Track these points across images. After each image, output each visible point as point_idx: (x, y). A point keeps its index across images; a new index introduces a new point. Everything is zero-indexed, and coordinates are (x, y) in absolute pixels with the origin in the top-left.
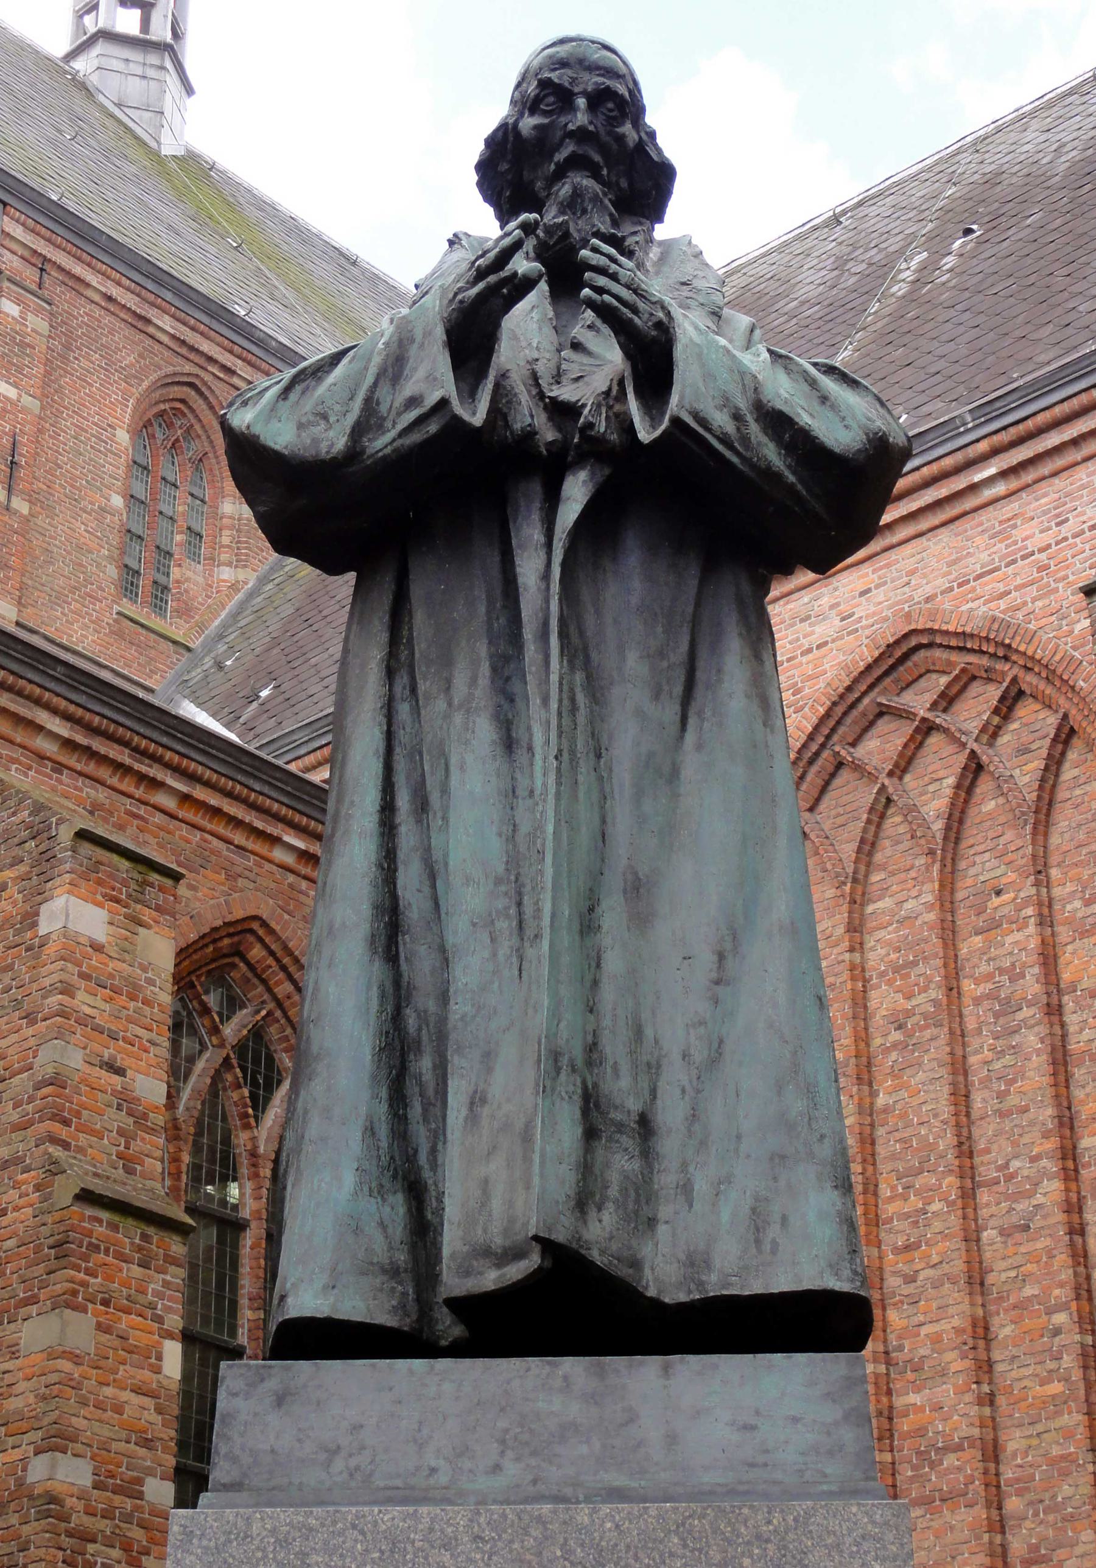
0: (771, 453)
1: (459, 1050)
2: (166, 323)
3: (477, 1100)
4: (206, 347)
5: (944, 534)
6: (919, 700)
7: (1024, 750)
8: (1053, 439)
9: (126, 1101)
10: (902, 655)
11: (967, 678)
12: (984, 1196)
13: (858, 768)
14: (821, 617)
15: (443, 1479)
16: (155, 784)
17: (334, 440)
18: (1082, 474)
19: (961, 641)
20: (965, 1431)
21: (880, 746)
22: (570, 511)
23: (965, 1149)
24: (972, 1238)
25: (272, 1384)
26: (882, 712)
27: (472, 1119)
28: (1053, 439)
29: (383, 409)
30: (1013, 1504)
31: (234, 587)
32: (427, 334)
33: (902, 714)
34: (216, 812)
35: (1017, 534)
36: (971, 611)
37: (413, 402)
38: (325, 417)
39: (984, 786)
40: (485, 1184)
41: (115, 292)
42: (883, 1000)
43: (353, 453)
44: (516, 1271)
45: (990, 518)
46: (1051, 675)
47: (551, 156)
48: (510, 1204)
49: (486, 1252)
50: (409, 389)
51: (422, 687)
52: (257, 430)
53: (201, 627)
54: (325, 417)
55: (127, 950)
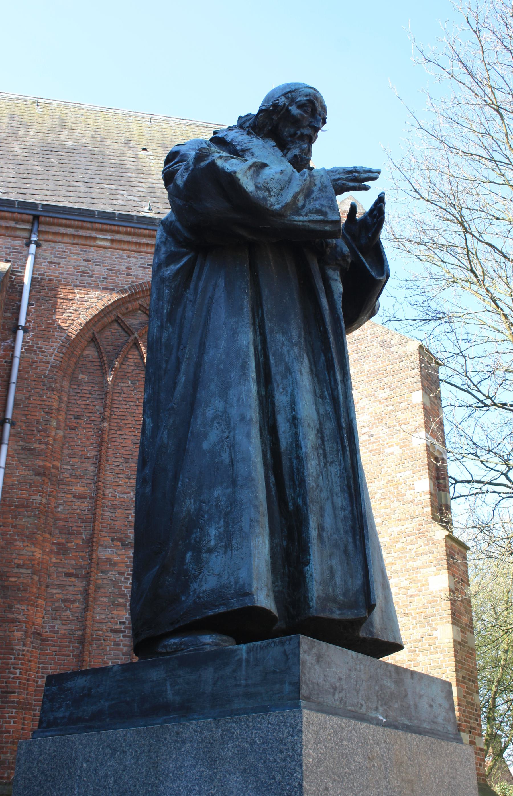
3: (321, 528)
15: (364, 710)
17: (275, 203)
25: (315, 650)
27: (320, 536)
29: (300, 204)
37: (319, 212)
38: (269, 190)
40: (331, 570)
43: (279, 214)
47: (299, 128)
48: (345, 582)
49: (335, 600)
51: (268, 325)
52: (239, 176)
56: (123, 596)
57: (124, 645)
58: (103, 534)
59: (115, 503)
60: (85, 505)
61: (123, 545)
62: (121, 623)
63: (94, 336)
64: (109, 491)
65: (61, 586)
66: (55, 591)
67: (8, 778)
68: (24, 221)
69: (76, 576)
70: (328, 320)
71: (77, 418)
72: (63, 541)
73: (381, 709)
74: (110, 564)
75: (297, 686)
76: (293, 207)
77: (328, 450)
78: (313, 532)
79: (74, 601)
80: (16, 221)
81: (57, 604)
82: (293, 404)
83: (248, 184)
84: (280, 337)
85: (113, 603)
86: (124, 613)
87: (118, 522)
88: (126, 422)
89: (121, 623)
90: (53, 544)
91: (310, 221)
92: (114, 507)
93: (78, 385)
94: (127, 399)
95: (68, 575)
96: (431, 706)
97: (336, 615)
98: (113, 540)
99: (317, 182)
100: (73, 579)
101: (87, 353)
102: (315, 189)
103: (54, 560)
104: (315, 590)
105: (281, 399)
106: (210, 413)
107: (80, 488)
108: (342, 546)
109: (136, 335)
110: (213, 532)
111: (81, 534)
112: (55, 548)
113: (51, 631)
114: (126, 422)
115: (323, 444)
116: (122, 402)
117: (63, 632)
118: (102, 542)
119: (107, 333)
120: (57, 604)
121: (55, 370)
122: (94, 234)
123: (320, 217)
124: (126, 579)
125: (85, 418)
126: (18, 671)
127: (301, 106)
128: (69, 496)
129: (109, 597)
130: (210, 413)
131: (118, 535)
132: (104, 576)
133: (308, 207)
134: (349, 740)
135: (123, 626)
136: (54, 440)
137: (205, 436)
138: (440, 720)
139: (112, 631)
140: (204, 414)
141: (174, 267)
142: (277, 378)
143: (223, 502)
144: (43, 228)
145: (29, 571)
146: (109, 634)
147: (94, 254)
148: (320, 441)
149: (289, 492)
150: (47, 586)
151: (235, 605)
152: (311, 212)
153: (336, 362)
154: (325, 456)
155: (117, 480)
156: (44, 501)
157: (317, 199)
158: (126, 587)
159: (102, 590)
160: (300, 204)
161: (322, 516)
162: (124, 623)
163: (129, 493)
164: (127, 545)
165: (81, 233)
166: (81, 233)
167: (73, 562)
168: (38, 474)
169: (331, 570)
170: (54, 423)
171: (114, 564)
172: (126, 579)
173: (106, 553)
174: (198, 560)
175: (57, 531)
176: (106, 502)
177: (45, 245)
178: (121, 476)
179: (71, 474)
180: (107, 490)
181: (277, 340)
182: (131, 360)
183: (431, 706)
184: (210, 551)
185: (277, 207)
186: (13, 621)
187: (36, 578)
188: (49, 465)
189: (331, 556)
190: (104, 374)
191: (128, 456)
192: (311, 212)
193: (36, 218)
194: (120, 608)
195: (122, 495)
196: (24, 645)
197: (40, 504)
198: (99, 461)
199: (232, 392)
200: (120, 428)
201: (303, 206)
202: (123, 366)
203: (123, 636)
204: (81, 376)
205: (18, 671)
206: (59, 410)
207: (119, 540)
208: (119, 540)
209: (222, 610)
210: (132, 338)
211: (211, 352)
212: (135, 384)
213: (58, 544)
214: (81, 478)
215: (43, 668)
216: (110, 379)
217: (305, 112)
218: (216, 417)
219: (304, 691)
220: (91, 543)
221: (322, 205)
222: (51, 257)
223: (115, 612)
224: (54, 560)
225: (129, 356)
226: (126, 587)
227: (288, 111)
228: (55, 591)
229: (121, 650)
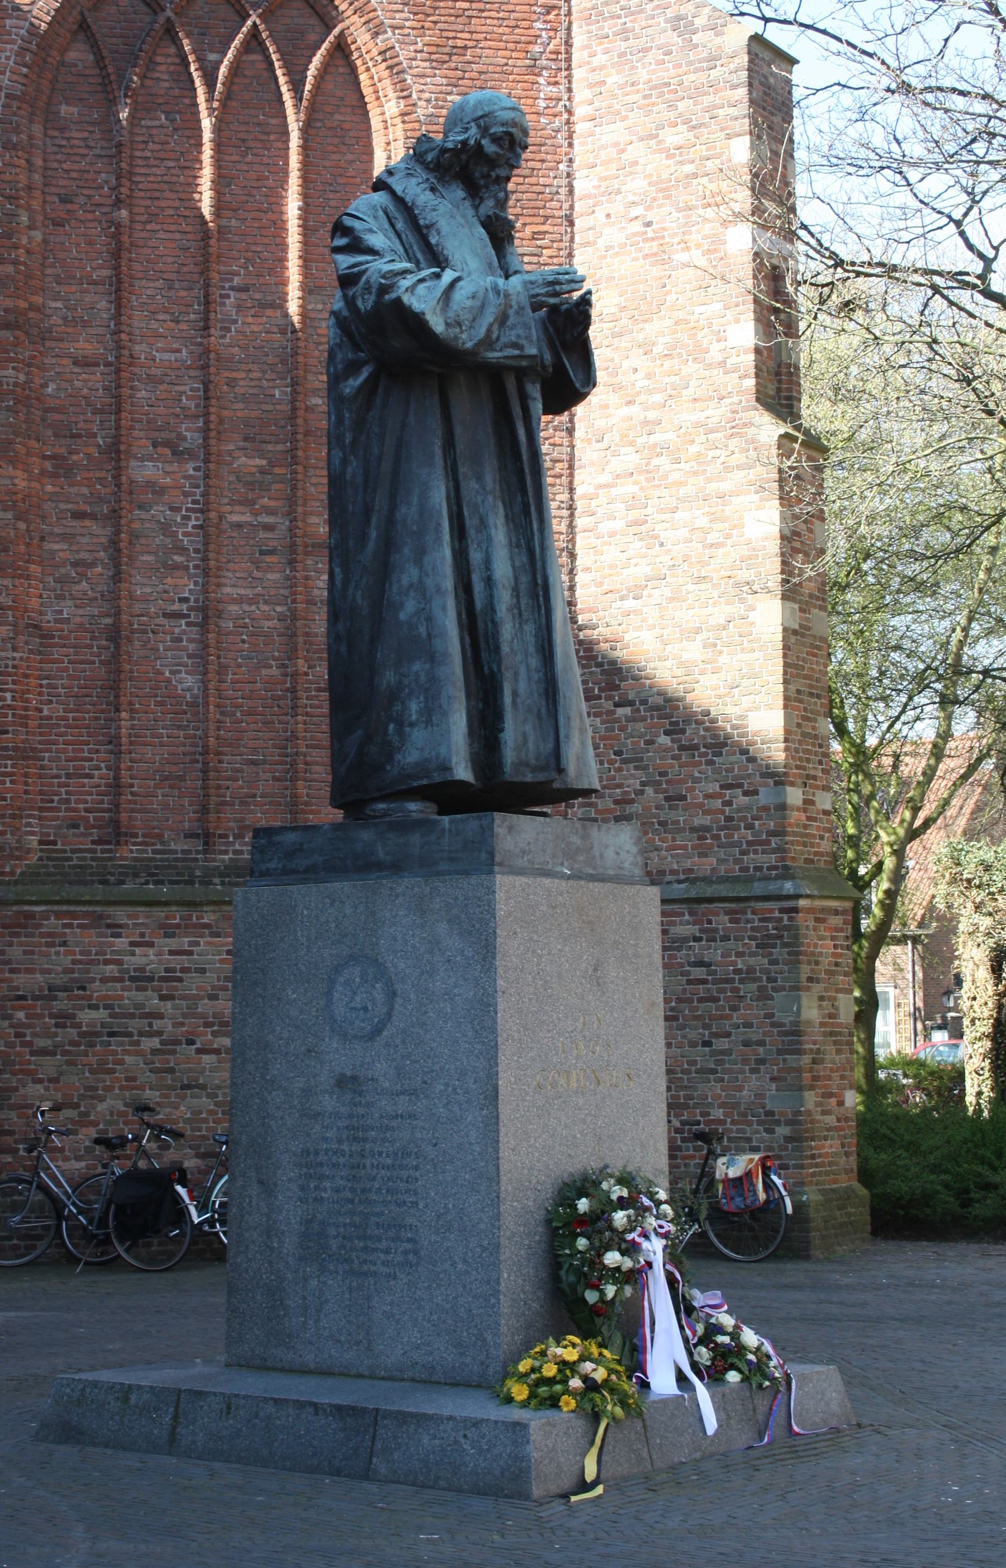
1: (507, 669)
3: (515, 694)
15: (550, 867)
17: (467, 340)
25: (507, 823)
27: (514, 703)
29: (494, 336)
32: (522, 308)
37: (515, 345)
40: (525, 735)
43: (473, 353)
49: (527, 764)
51: (462, 470)
52: (428, 317)
54: (459, 324)
56: (182, 550)
57: (191, 641)
58: (136, 433)
59: (154, 371)
60: (97, 379)
61: (174, 453)
62: (182, 600)
63: (84, 20)
65: (66, 538)
66: (56, 547)
67: (12, 873)
69: (93, 516)
70: (525, 456)
71: (65, 200)
72: (63, 451)
73: (566, 863)
74: (154, 492)
75: (492, 854)
76: (488, 342)
77: (523, 606)
78: (508, 700)
79: (93, 565)
81: (63, 571)
82: (488, 562)
83: (437, 324)
84: (474, 484)
85: (165, 564)
86: (185, 580)
87: (162, 410)
88: (163, 204)
89: (182, 600)
90: (45, 458)
91: (505, 357)
92: (153, 380)
93: (62, 129)
94: (162, 155)
95: (78, 515)
96: (618, 854)
97: (529, 778)
98: (155, 445)
99: (514, 303)
100: (87, 523)
101: (72, 55)
102: (511, 312)
103: (49, 488)
104: (509, 756)
105: (476, 557)
106: (405, 581)
107: (84, 345)
108: (535, 710)
109: (169, 13)
110: (414, 707)
111: (95, 435)
112: (48, 465)
113: (56, 621)
114: (163, 204)
115: (519, 602)
116: (152, 162)
117: (78, 620)
118: (135, 449)
120: (63, 571)
121: (15, 104)
123: (516, 352)
124: (184, 518)
125: (82, 200)
126: (8, 695)
127: (496, 139)
128: (65, 361)
129: (156, 553)
130: (405, 581)
131: (165, 435)
132: (143, 515)
133: (504, 339)
134: (534, 894)
135: (185, 606)
136: (28, 252)
137: (402, 605)
138: (627, 865)
139: (166, 615)
140: (399, 581)
141: (354, 383)
142: (471, 533)
143: (423, 678)
145: (9, 515)
146: (162, 620)
148: (515, 601)
149: (484, 655)
150: (42, 539)
151: (437, 778)
152: (506, 346)
153: (533, 508)
154: (520, 614)
155: (154, 325)
156: (22, 378)
157: (513, 327)
158: (186, 534)
159: (143, 541)
160: (494, 336)
161: (516, 681)
162: (186, 600)
163: (179, 351)
164: (182, 453)
167: (85, 490)
169: (525, 735)
170: (24, 219)
171: (161, 491)
172: (184, 518)
173: (145, 470)
174: (400, 732)
175: (49, 432)
176: (137, 370)
178: (161, 317)
179: (65, 318)
180: (137, 347)
181: (470, 487)
182: (163, 68)
183: (618, 854)
184: (412, 725)
185: (469, 345)
187: (22, 525)
188: (23, 304)
189: (525, 721)
190: (111, 104)
191: (174, 276)
192: (506, 346)
194: (178, 573)
195: (166, 356)
196: (15, 649)
197: (16, 384)
198: (118, 291)
199: (426, 559)
200: (153, 217)
201: (498, 339)
202: (148, 82)
203: (188, 624)
204: (64, 110)
205: (8, 695)
206: (29, 188)
207: (167, 444)
208: (167, 444)
209: (425, 782)
210: (162, 19)
211: (403, 509)
212: (174, 120)
213: (53, 457)
214: (86, 324)
215: (50, 686)
216: (124, 115)
217: (501, 147)
218: (411, 586)
219: (498, 858)
220: (116, 453)
221: (518, 336)
223: (169, 580)
224: (49, 488)
225: (159, 59)
226: (186, 534)
227: (479, 145)
228: (56, 547)
229: (185, 649)
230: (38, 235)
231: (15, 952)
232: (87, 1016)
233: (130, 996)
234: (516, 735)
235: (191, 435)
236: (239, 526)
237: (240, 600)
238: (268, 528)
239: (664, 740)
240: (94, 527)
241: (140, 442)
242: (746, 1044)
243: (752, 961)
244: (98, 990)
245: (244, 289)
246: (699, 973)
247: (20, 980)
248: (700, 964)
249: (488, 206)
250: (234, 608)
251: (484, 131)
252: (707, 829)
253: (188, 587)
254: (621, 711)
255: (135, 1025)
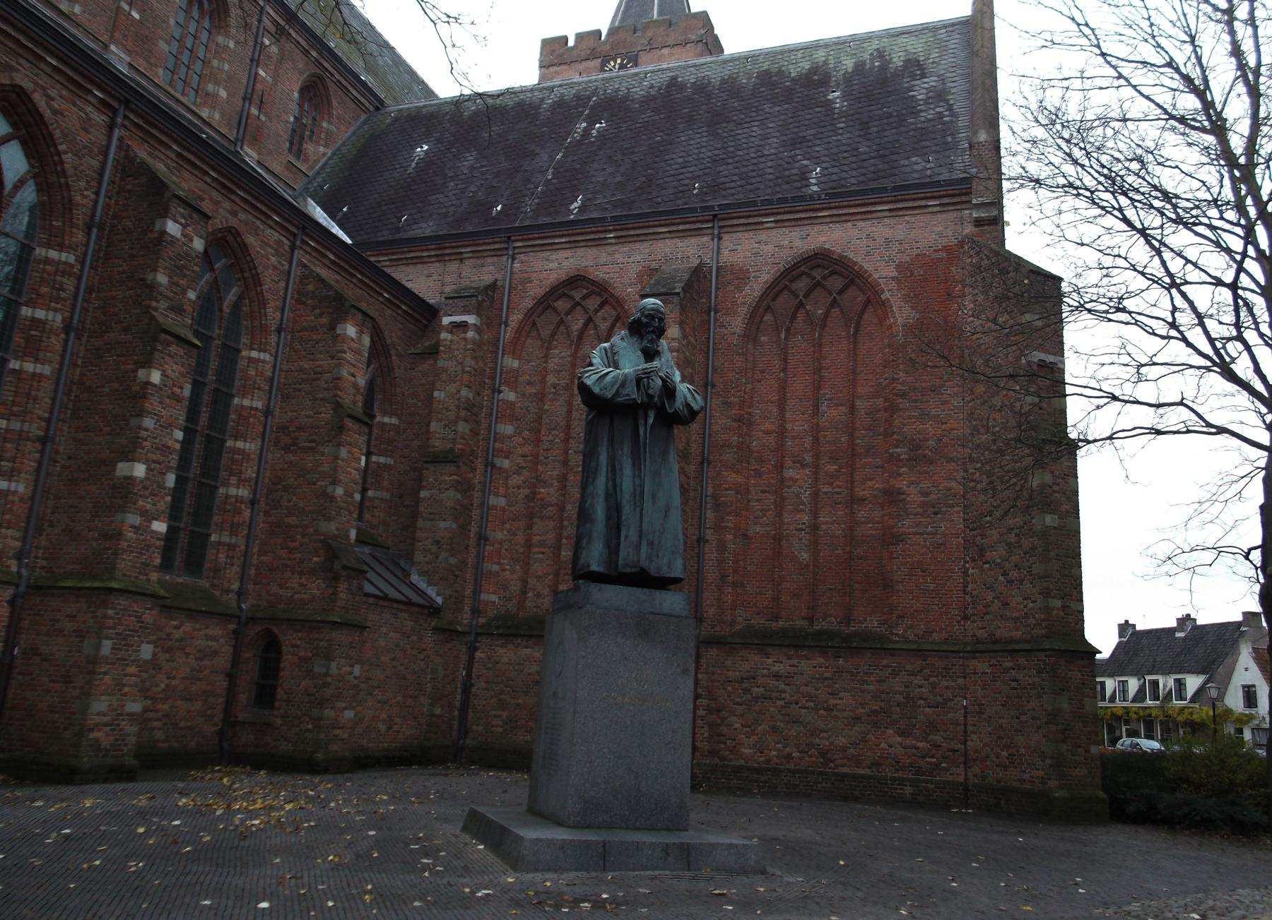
0: (686, 412)
2: (314, 54)
3: (627, 536)
4: (326, 65)
5: (594, 249)
6: (577, 296)
7: (605, 319)
8: (632, 232)
9: (355, 385)
10: (576, 280)
11: (592, 293)
12: (571, 441)
13: (555, 310)
14: (552, 261)
16: (353, 276)
17: (609, 395)
18: (638, 245)
19: (593, 282)
20: (555, 501)
21: (562, 305)
22: (651, 421)
23: (568, 427)
24: (566, 452)
26: (565, 295)
28: (632, 232)
30: (566, 523)
31: (324, 154)
33: (572, 298)
34: (368, 285)
35: (617, 256)
36: (599, 274)
39: (591, 325)
41: (300, 39)
42: (551, 379)
44: (634, 570)
45: (609, 249)
46: (617, 300)
50: (626, 392)
53: (312, 168)
55: (359, 339)
56: (804, 504)
64: (789, 426)
68: (707, 221)
71: (762, 372)
76: (617, 394)
80: (702, 222)
83: (596, 390)
92: (793, 438)
95: (763, 492)
97: (628, 570)
104: (621, 562)
105: (618, 481)
107: (767, 426)
119: (780, 299)
122: (760, 219)
127: (646, 317)
144: (722, 224)
147: (763, 235)
165: (751, 220)
166: (751, 220)
168: (735, 420)
173: (790, 473)
177: (725, 237)
186: (725, 528)
190: (779, 333)
193: (715, 216)
204: (763, 339)
208: (799, 462)
220: (780, 467)
222: (731, 246)
230: (749, 386)
231: (729, 663)
232: (756, 691)
233: (772, 683)
234: (626, 554)
235: (808, 458)
236: (826, 493)
237: (827, 523)
238: (838, 493)
239: (1001, 578)
240: (769, 496)
241: (788, 462)
242: (1034, 718)
243: (1035, 679)
244: (760, 680)
245: (830, 399)
246: (1014, 684)
247: (730, 673)
248: (1014, 680)
249: (645, 343)
250: (824, 527)
251: (643, 314)
252: (1017, 618)
253: (806, 518)
254: (987, 566)
255: (774, 695)
